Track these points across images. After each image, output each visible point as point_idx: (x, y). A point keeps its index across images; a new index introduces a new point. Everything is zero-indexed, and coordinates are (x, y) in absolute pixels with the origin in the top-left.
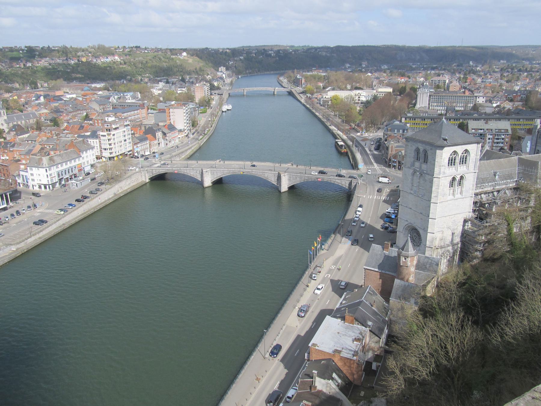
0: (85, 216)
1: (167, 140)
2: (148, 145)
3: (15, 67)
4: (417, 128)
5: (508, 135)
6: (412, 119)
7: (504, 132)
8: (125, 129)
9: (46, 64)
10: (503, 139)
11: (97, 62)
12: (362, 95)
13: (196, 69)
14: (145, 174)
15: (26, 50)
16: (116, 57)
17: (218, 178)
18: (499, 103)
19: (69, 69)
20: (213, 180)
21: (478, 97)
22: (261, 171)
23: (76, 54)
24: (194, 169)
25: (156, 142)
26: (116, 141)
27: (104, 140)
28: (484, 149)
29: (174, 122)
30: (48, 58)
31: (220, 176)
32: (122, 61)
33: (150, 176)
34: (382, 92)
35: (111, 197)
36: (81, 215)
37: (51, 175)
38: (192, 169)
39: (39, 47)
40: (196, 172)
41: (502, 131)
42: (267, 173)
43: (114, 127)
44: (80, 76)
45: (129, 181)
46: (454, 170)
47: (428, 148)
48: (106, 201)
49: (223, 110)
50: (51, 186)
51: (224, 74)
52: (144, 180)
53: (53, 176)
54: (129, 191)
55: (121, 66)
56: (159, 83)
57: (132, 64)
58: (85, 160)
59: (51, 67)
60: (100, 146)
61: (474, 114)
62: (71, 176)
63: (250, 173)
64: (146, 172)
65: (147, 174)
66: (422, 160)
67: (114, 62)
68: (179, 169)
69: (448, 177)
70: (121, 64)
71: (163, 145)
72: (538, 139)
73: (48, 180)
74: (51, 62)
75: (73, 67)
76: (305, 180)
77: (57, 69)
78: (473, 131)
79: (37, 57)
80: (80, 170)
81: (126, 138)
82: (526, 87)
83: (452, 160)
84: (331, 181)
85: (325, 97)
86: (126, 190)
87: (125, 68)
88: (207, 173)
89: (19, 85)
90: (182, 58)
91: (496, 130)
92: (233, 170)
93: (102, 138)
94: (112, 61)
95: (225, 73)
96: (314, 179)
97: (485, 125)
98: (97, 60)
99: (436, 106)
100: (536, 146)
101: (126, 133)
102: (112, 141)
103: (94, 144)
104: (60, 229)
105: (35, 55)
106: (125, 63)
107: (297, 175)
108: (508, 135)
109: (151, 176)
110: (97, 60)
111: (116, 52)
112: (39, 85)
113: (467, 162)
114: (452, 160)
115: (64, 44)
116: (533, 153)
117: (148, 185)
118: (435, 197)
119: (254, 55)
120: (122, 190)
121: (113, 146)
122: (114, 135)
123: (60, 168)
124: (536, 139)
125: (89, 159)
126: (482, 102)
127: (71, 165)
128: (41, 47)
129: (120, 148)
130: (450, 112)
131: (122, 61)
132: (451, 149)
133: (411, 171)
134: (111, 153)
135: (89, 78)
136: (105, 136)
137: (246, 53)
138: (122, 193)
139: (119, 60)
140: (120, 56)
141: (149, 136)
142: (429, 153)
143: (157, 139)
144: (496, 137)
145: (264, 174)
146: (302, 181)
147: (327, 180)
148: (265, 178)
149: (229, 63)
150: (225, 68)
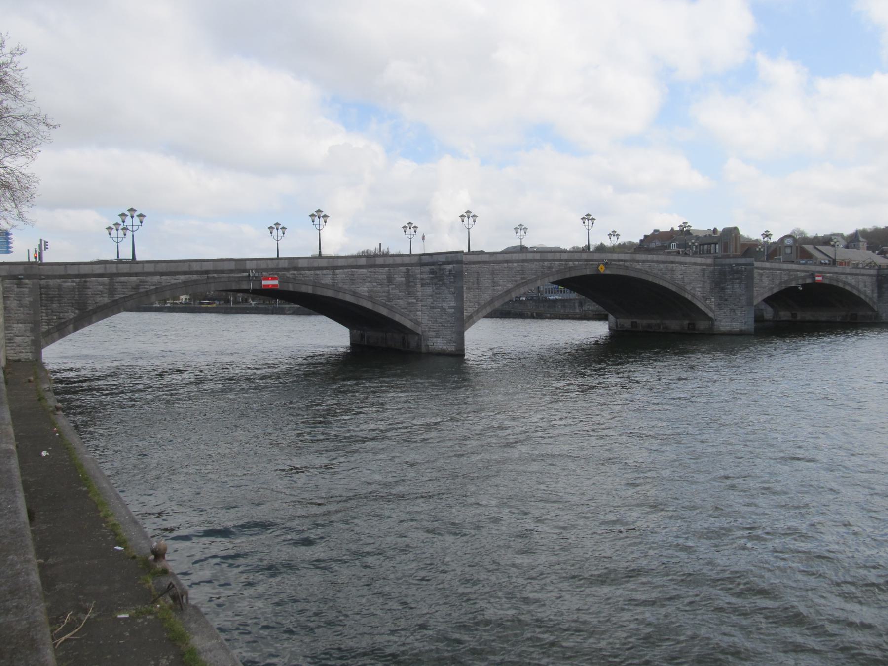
31: (508, 292)
40: (390, 280)
42: (680, 263)
76: (781, 283)
84: (838, 281)
96: (804, 278)
145: (672, 271)
146: (775, 290)
147: (831, 279)
148: (674, 288)
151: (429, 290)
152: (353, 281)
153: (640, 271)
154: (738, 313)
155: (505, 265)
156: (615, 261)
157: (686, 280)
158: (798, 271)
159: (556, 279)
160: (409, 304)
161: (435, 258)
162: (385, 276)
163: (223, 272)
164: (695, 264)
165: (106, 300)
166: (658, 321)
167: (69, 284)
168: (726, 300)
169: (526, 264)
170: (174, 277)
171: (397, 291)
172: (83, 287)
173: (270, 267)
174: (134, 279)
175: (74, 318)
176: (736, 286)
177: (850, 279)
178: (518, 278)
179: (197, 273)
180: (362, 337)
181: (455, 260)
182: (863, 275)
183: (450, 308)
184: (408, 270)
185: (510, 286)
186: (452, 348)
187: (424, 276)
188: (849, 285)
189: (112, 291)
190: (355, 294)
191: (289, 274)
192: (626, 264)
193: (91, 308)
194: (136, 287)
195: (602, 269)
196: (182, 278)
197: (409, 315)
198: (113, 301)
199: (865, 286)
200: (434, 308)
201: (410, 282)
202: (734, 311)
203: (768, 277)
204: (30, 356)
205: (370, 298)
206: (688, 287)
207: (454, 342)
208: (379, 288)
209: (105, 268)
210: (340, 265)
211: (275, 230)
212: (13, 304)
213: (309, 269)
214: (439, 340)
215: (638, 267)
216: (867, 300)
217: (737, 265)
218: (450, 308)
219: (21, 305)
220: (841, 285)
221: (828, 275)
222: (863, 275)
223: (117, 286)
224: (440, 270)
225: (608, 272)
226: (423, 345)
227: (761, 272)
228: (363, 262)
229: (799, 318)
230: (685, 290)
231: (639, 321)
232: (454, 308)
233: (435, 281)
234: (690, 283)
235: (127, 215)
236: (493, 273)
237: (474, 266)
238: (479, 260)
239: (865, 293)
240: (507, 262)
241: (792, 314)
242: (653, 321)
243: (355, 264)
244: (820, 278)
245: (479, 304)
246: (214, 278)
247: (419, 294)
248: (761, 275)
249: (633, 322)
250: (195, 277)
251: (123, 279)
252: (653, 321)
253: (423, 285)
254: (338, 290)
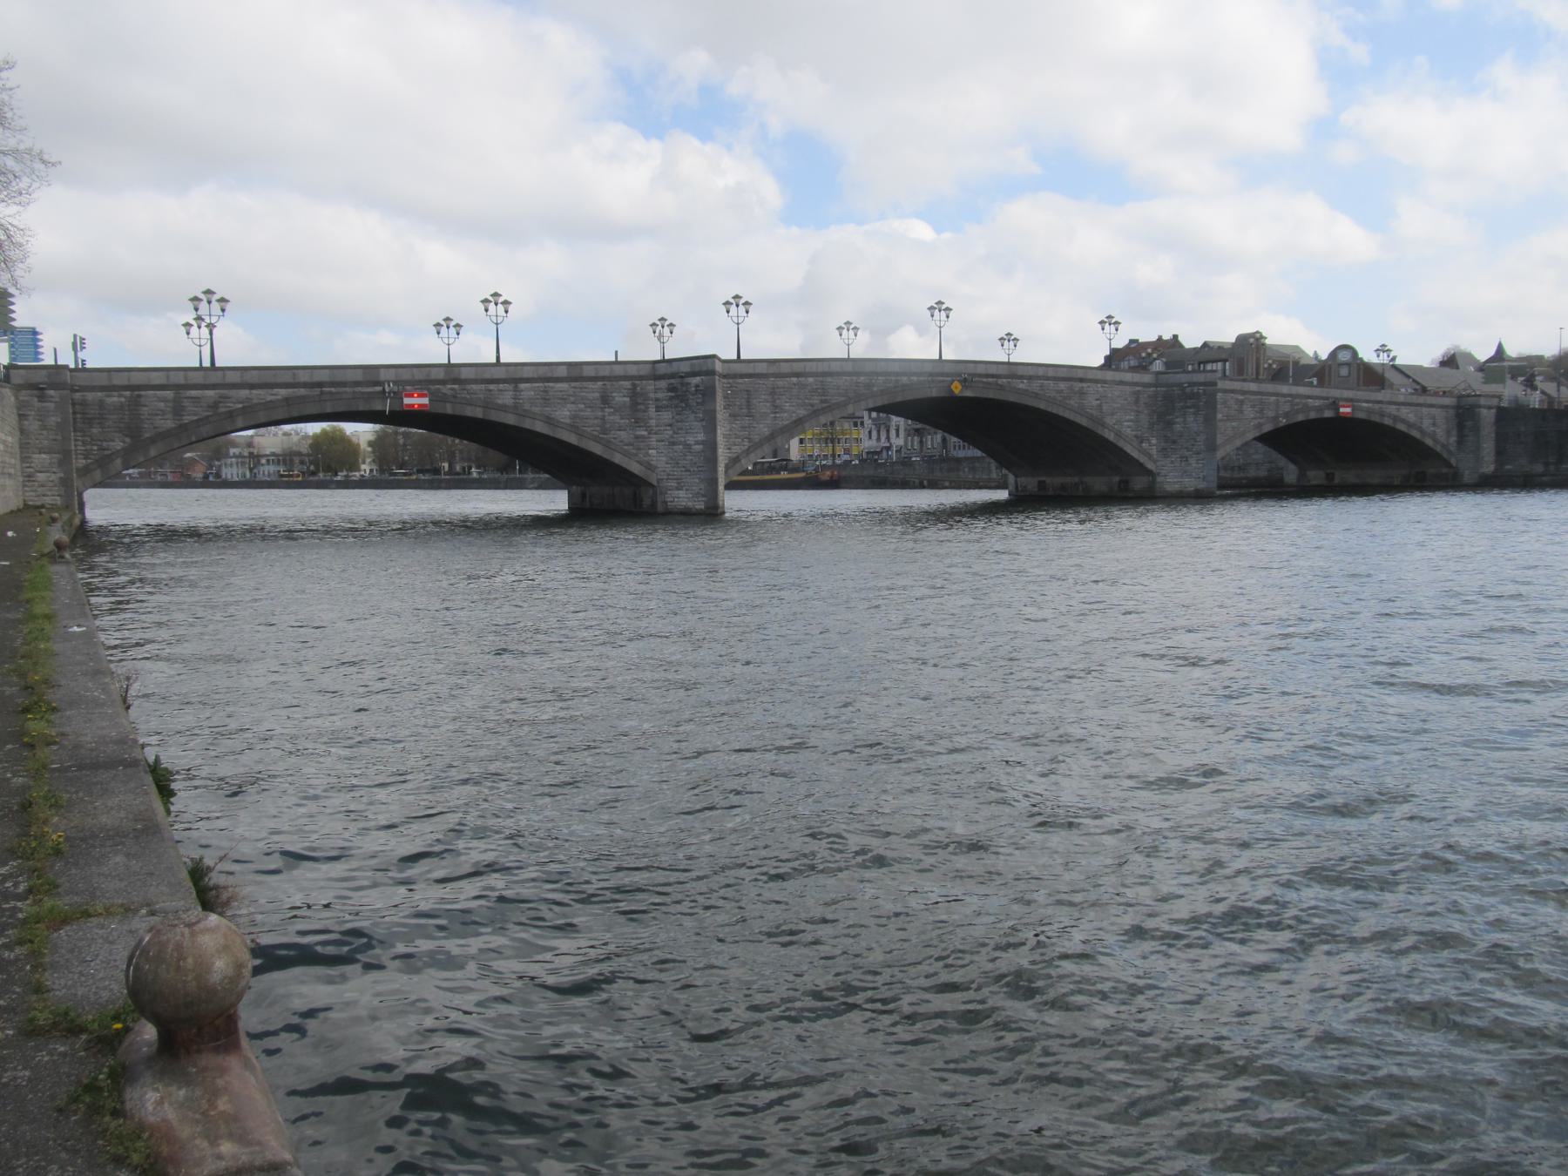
40: (605, 400)
63: (1001, 388)
84: (1382, 415)
96: (1319, 409)
145: (1082, 393)
147: (1369, 411)
148: (1084, 422)
151: (666, 416)
152: (546, 401)
153: (1025, 392)
154: (1193, 461)
155: (795, 380)
156: (980, 376)
157: (1105, 408)
158: (1309, 397)
159: (879, 404)
160: (637, 437)
161: (674, 368)
162: (597, 395)
163: (343, 384)
164: (1121, 383)
165: (169, 424)
166: (1076, 479)
167: (115, 399)
168: (1174, 442)
169: (829, 379)
170: (270, 391)
171: (616, 418)
172: (135, 403)
173: (417, 378)
174: (210, 393)
175: (123, 449)
176: (1190, 418)
177: (1405, 412)
178: (816, 400)
179: (305, 385)
180: (584, 495)
181: (704, 369)
182: (1432, 406)
183: (697, 443)
184: (635, 386)
185: (802, 412)
186: (700, 506)
187: (660, 395)
188: (1403, 421)
189: (178, 410)
190: (549, 421)
191: (447, 389)
192: (1000, 381)
193: (147, 435)
194: (215, 405)
195: (957, 389)
196: (283, 392)
197: (636, 455)
198: (181, 426)
199: (1434, 424)
200: (674, 444)
201: (638, 404)
202: (1185, 459)
203: (1253, 406)
204: (59, 501)
205: (574, 428)
206: (1109, 421)
207: (703, 496)
208: (588, 413)
209: (168, 377)
210: (525, 376)
211: (445, 328)
212: (33, 425)
213: (476, 381)
214: (682, 493)
215: (1021, 386)
216: (1438, 448)
217: (1192, 384)
218: (697, 443)
219: (44, 428)
220: (1387, 421)
221: (1365, 405)
222: (1432, 406)
223: (186, 403)
224: (682, 384)
225: (968, 393)
226: (659, 500)
227: (1241, 397)
228: (562, 372)
229: (1337, 481)
230: (1103, 425)
231: (1048, 480)
232: (702, 442)
233: (675, 402)
234: (1113, 414)
235: (201, 300)
237: (740, 381)
238: (751, 371)
239: (1433, 436)
240: (797, 375)
241: (1327, 475)
242: (1068, 480)
243: (549, 375)
244: (1349, 410)
245: (750, 440)
246: (330, 393)
247: (653, 422)
248: (1242, 402)
249: (1040, 482)
250: (302, 391)
251: (194, 393)
252: (1068, 480)
253: (658, 409)
254: (524, 414)
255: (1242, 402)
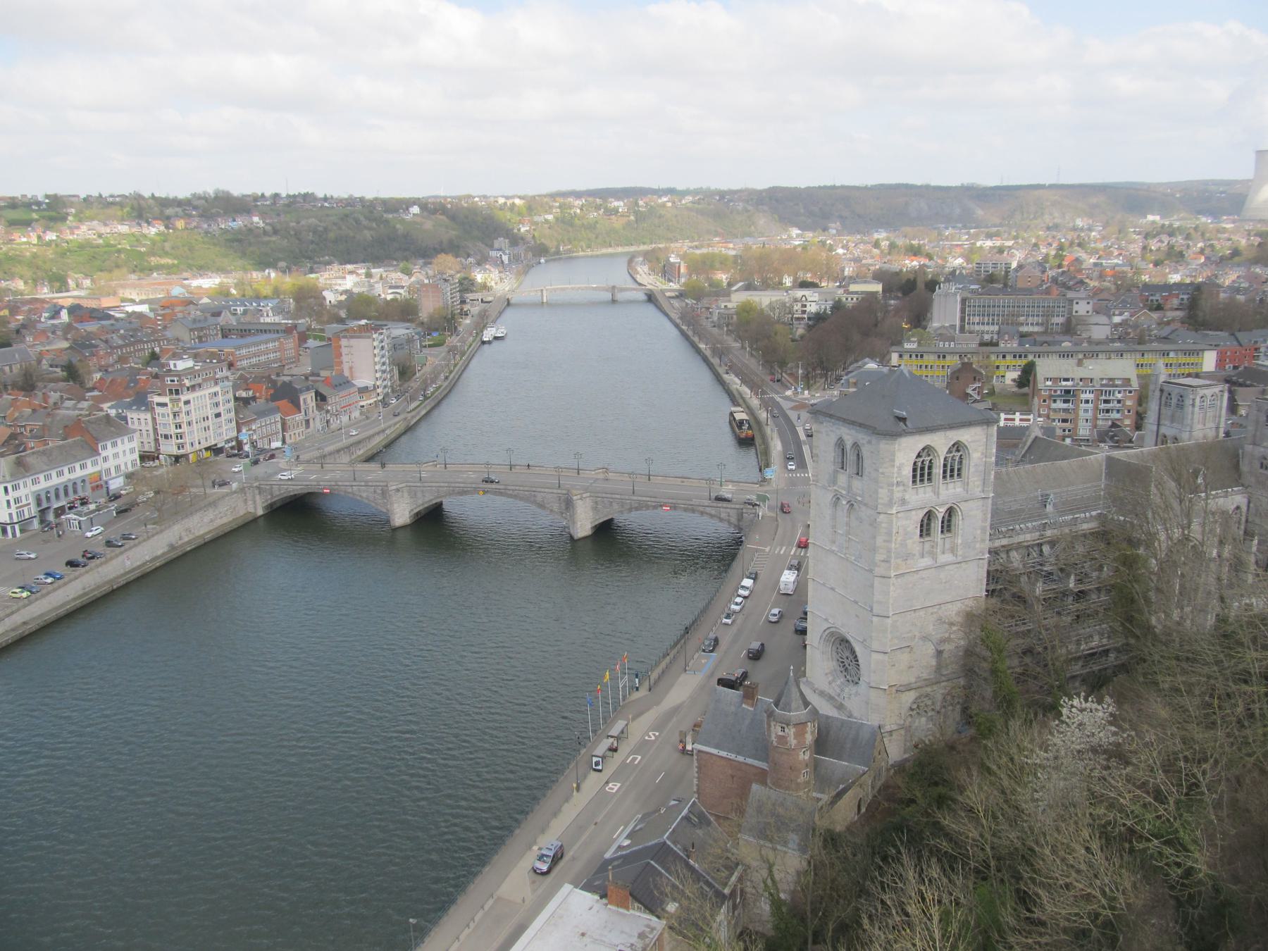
0: (84, 603)
1: (328, 411)
2: (279, 426)
3: (18, 241)
4: (927, 376)
5: (1130, 392)
6: (914, 356)
7: (1122, 386)
8: (217, 389)
9: (91, 236)
10: (1119, 402)
11: (211, 230)
12: (809, 299)
13: (441, 242)
14: (254, 497)
15: (47, 203)
16: (256, 219)
17: (426, 505)
18: (1126, 314)
19: (144, 246)
20: (415, 511)
21: (1075, 302)
22: (526, 489)
23: (162, 212)
24: (370, 484)
25: (299, 417)
26: (193, 417)
27: (163, 415)
28: (1029, 436)
29: (351, 368)
30: (95, 223)
31: (431, 500)
32: (268, 228)
33: (267, 501)
34: (856, 293)
35: (159, 553)
36: (74, 599)
37: (17, 500)
38: (363, 484)
39: (78, 196)
40: (375, 492)
41: (1117, 382)
43: (187, 383)
44: (170, 261)
45: (210, 514)
46: (932, 494)
47: (862, 438)
48: (144, 564)
49: (485, 339)
50: (17, 527)
51: (505, 254)
52: (252, 511)
53: (24, 502)
54: (208, 537)
55: (266, 239)
56: (345, 278)
57: (292, 233)
58: (111, 464)
59: (101, 241)
60: (155, 430)
61: (1063, 342)
62: (73, 502)
64: (257, 492)
65: (258, 497)
66: (851, 469)
67: (250, 230)
68: (333, 483)
69: (914, 513)
70: (265, 233)
71: (317, 424)
72: (1162, 407)
73: (10, 515)
74: (103, 230)
75: (154, 243)
77: (115, 246)
78: (1049, 383)
79: (70, 218)
80: (97, 486)
81: (221, 409)
82: (1195, 276)
83: (922, 469)
85: (726, 306)
86: (202, 536)
87: (274, 242)
88: (400, 493)
89: (26, 283)
90: (408, 217)
91: (1102, 379)
92: (462, 485)
93: (158, 410)
94: (245, 226)
95: (507, 252)
97: (1076, 368)
98: (210, 225)
99: (978, 324)
100: (1159, 425)
101: (220, 398)
102: (183, 418)
103: (140, 423)
104: (13, 634)
105: (68, 214)
106: (275, 232)
107: (614, 496)
108: (1130, 392)
109: (269, 502)
110: (210, 225)
111: (257, 206)
112: (71, 283)
113: (964, 472)
114: (922, 469)
115: (137, 190)
116: (1154, 442)
117: (261, 522)
118: (883, 561)
119: (578, 211)
120: (191, 537)
121: (185, 428)
122: (187, 402)
123: (43, 484)
124: (1157, 408)
125: (121, 461)
126: (1085, 313)
127: (73, 476)
128: (83, 196)
129: (204, 434)
130: (1006, 337)
131: (268, 228)
132: (920, 442)
133: (829, 496)
134: (180, 446)
135: (190, 267)
136: (165, 405)
137: (560, 207)
138: (189, 542)
139: (261, 224)
140: (263, 215)
141: (283, 403)
142: (865, 452)
143: (303, 413)
144: (1104, 397)
145: (535, 496)
149: (519, 230)
150: (507, 241)
172: (272, 488)
185: (432, 498)
199: (729, 516)
205: (367, 498)
236: (422, 491)
248: (611, 502)
254: (354, 494)
255: (611, 502)
